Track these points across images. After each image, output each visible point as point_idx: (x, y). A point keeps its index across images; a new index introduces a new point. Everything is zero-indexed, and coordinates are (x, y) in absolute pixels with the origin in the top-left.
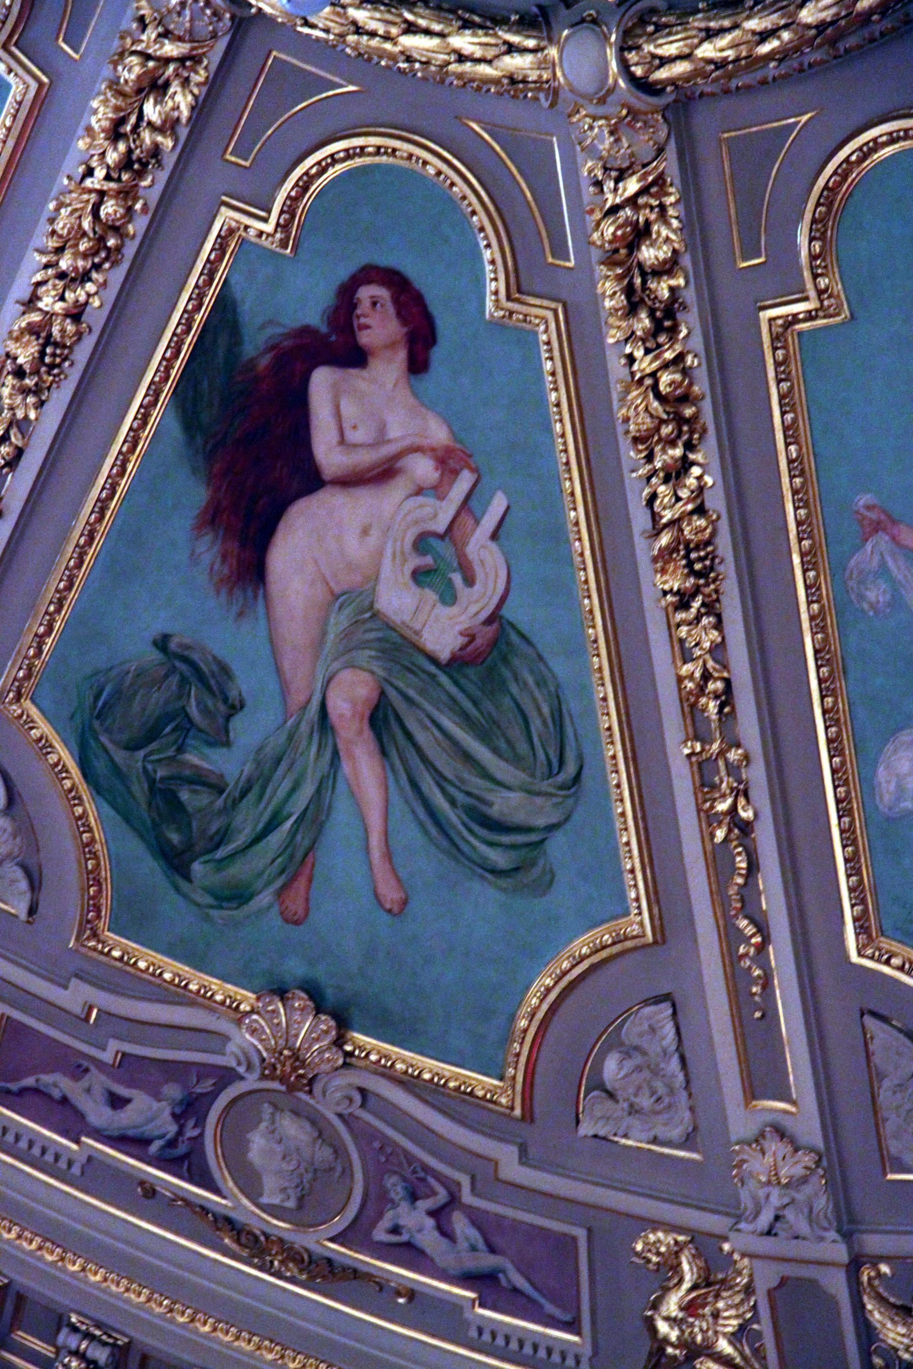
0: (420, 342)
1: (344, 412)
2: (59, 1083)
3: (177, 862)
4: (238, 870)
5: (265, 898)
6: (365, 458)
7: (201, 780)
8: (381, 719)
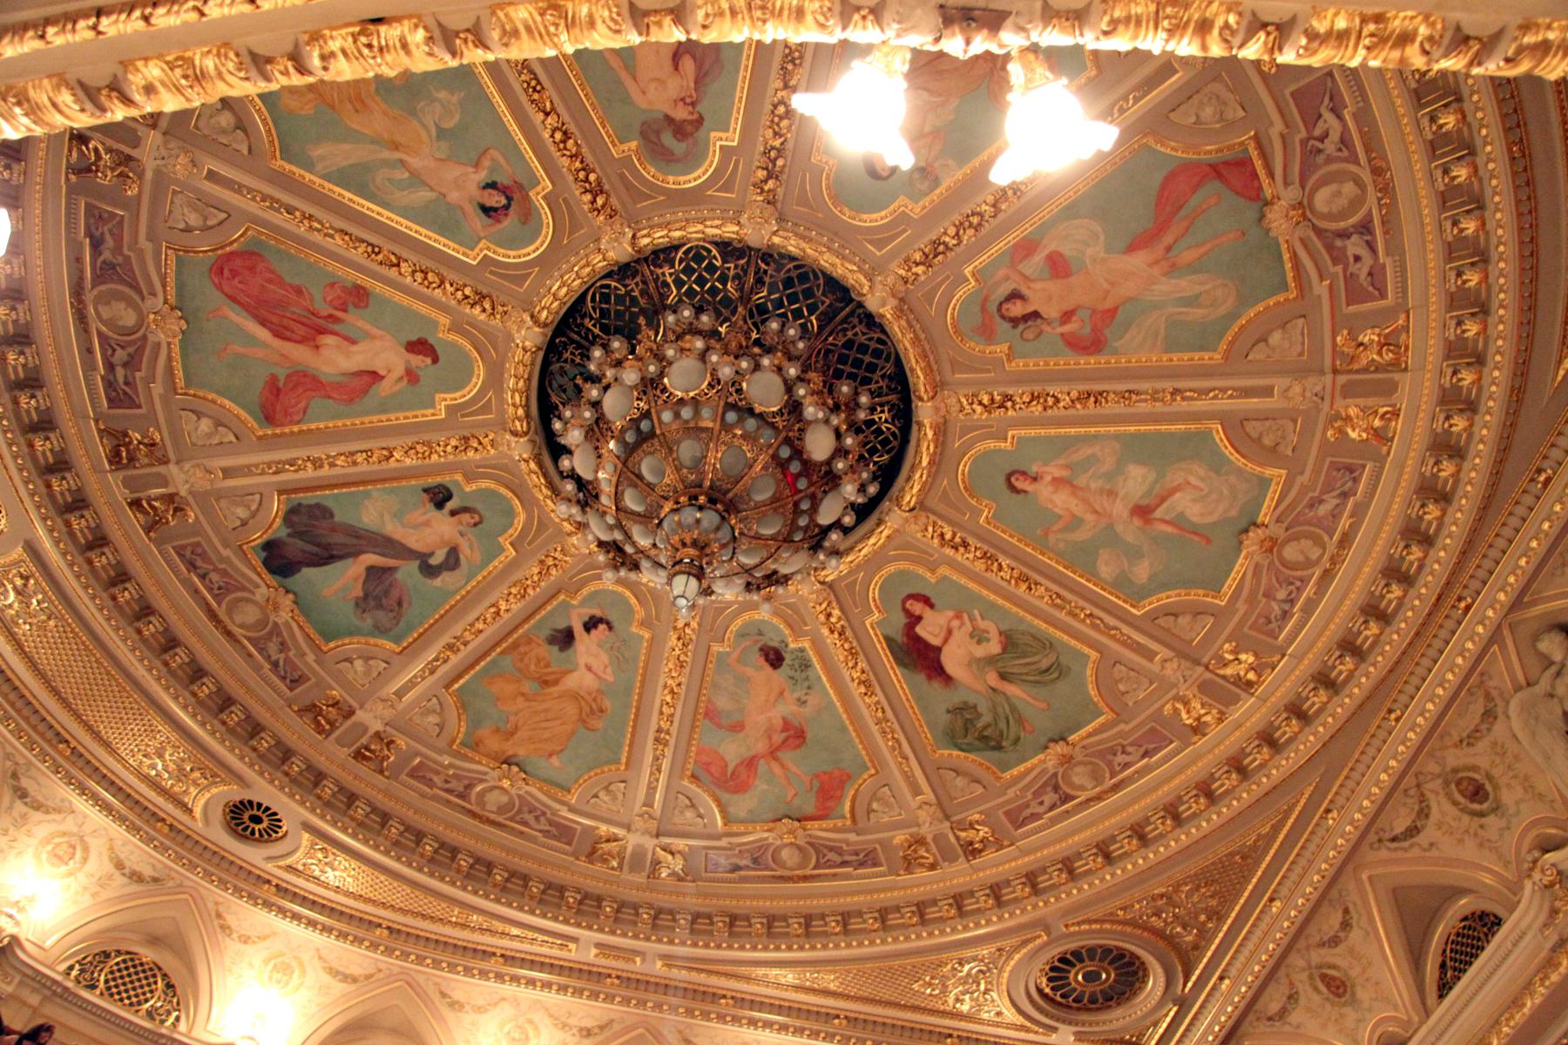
0: (927, 601)
1: (929, 631)
2: (1027, 813)
3: (999, 748)
4: (1012, 736)
6: (943, 634)
7: (985, 727)
8: (1003, 676)
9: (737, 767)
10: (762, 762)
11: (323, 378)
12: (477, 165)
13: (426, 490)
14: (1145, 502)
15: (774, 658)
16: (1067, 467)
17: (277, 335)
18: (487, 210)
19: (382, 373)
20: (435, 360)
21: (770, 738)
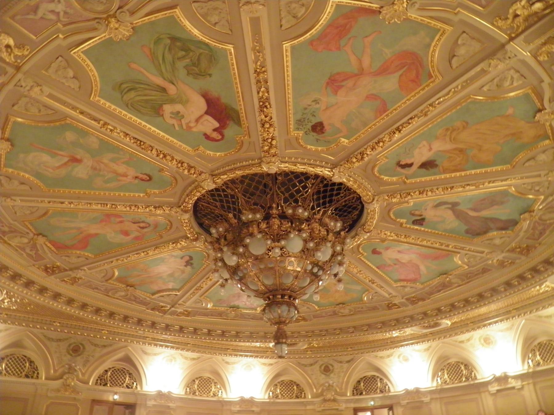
1: (210, 124)
3: (174, 39)
5: (152, 46)
6: (201, 121)
7: (183, 57)
9: (394, 72)
14: (75, 164)
15: (318, 128)
16: (120, 181)
21: (354, 85)
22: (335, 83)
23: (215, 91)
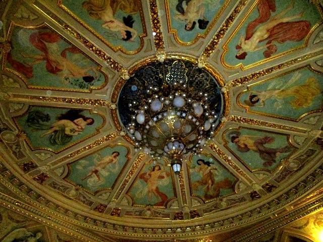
7: (38, 122)
8: (56, 131)
10: (44, 54)
11: (261, 24)
12: (263, 102)
13: (208, 22)
16: (115, 163)
17: (282, 24)
18: (254, 96)
19: (246, 41)
20: (237, 57)
22: (53, 70)
23: (59, 113)
